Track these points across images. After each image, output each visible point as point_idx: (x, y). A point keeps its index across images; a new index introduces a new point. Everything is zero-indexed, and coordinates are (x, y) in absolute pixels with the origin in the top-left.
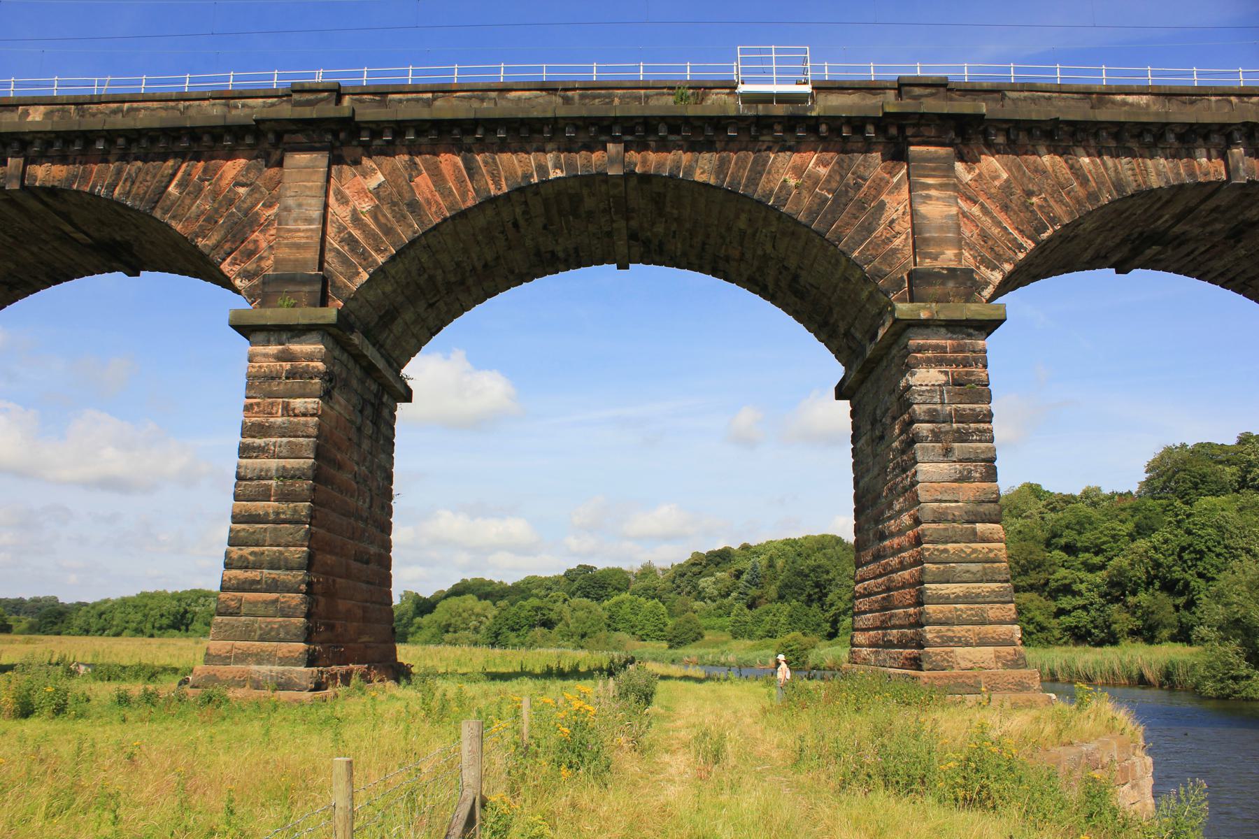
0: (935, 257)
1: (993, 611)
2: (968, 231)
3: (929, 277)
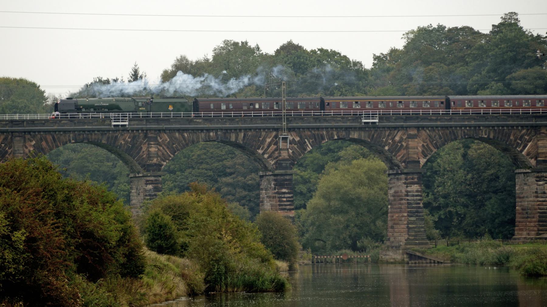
0: (152, 160)
2: (160, 153)
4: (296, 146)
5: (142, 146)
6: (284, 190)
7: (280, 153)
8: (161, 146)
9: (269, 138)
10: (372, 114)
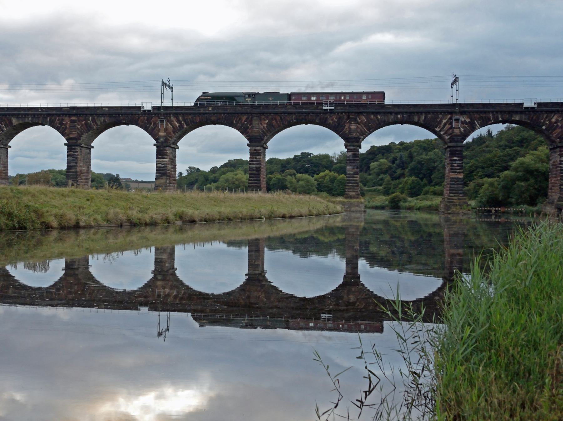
3: (351, 138)
4: (466, 126)
6: (455, 158)
7: (453, 130)
8: (360, 125)
9: (445, 119)
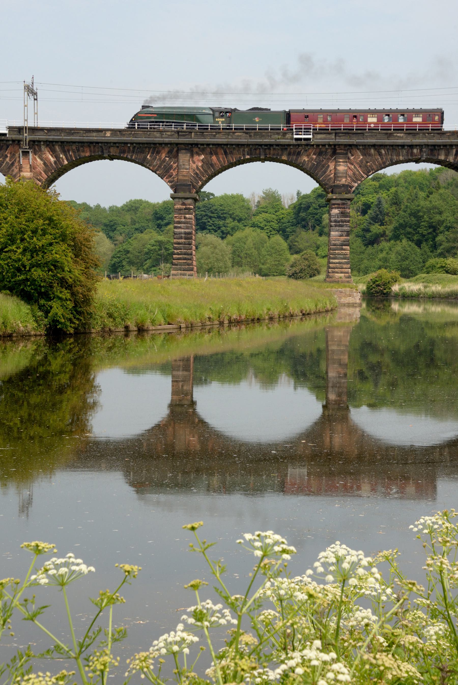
0: (340, 181)
1: (345, 266)
3: (338, 186)
5: (329, 164)
8: (352, 164)
10: (305, 129)
